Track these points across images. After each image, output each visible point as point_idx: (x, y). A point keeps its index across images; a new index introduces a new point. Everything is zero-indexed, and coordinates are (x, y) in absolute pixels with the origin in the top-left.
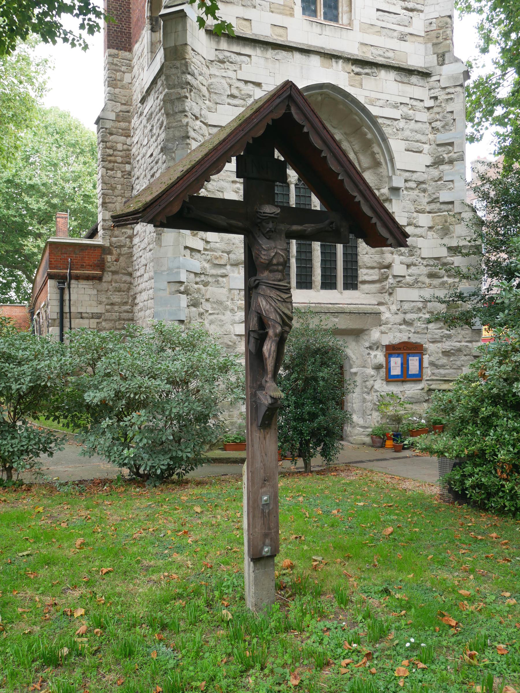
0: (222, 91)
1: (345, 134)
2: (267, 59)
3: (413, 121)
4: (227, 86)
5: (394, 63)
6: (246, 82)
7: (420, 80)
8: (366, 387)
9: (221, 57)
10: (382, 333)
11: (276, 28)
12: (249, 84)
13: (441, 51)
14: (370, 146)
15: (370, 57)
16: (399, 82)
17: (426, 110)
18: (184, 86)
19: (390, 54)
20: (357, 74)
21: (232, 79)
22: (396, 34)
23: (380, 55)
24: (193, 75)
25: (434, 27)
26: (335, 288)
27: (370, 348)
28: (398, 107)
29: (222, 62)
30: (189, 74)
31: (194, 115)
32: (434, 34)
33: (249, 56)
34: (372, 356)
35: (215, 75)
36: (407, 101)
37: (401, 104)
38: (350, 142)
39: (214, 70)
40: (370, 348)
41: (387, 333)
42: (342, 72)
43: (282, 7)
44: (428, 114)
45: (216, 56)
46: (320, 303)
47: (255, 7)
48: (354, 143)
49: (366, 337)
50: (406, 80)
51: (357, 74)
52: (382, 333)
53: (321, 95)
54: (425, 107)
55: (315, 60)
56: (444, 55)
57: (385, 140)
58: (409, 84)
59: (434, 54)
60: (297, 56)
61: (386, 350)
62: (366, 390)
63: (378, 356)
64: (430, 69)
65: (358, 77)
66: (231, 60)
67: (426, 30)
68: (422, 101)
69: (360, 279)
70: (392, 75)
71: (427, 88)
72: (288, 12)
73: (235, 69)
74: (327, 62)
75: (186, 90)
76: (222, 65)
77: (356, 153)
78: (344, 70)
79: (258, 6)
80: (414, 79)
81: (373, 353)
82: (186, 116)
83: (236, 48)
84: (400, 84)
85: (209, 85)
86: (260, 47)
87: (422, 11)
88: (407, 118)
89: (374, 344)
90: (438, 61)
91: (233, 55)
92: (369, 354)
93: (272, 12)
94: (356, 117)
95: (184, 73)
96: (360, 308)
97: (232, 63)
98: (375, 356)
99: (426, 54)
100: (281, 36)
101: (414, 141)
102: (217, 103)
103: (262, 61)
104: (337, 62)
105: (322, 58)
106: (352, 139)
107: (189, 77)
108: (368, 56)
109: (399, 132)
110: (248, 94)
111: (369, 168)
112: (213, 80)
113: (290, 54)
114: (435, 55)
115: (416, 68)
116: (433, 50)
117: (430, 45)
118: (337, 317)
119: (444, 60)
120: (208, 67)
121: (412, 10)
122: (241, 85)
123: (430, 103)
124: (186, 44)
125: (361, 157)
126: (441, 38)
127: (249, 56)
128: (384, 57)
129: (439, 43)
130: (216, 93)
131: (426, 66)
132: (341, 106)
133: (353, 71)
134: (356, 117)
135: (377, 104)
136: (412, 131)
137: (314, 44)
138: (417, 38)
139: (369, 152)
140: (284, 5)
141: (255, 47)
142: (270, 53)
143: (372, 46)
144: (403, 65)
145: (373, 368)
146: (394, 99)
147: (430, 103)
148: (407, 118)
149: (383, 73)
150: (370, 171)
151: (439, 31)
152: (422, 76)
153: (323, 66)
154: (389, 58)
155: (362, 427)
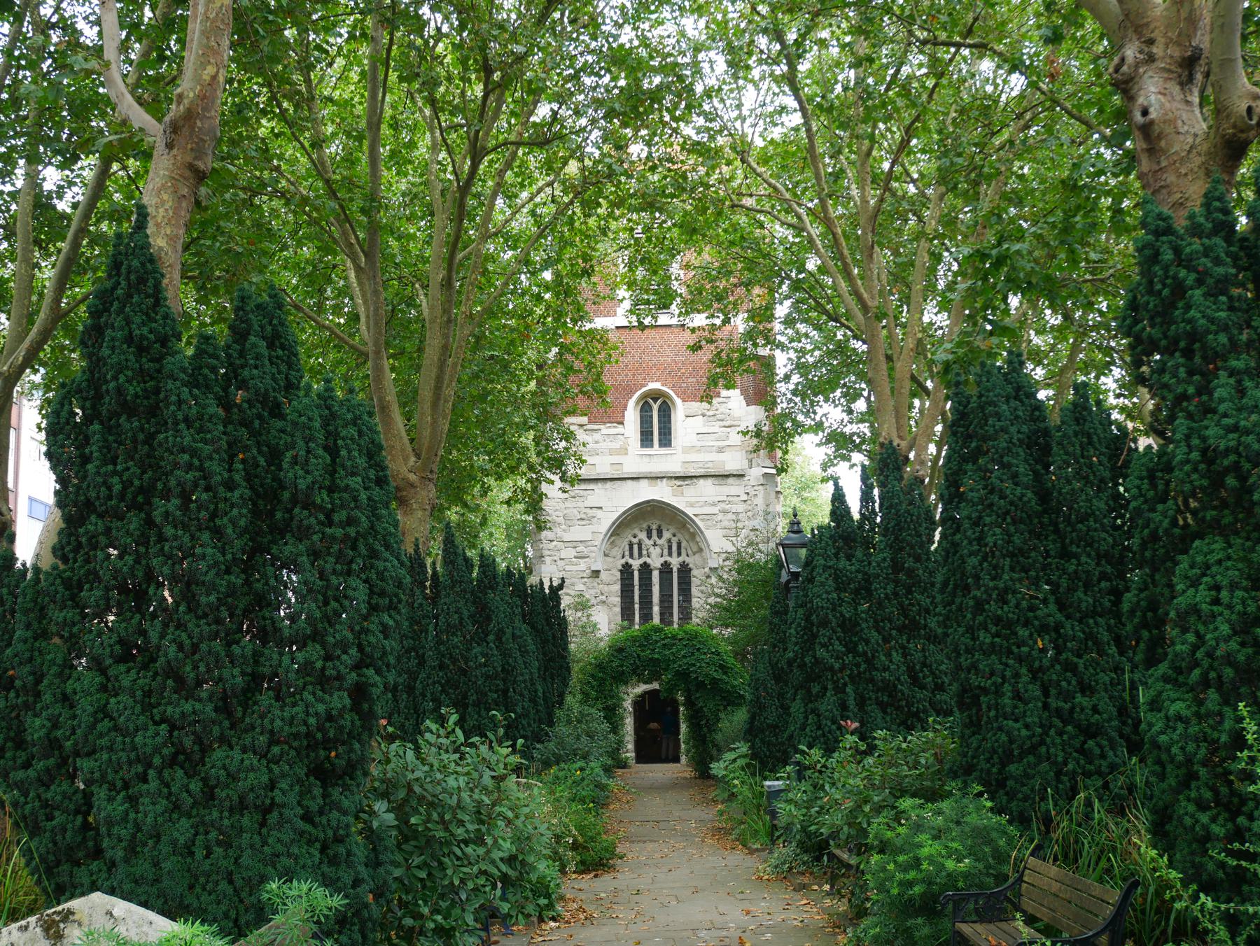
19: (710, 465)
39: (568, 504)
55: (644, 483)
60: (630, 482)
70: (710, 481)
74: (654, 482)
80: (731, 480)
88: (724, 512)
122: (588, 511)
123: (744, 497)
142: (609, 484)
146: (710, 500)
147: (744, 497)
148: (724, 512)
149: (702, 481)
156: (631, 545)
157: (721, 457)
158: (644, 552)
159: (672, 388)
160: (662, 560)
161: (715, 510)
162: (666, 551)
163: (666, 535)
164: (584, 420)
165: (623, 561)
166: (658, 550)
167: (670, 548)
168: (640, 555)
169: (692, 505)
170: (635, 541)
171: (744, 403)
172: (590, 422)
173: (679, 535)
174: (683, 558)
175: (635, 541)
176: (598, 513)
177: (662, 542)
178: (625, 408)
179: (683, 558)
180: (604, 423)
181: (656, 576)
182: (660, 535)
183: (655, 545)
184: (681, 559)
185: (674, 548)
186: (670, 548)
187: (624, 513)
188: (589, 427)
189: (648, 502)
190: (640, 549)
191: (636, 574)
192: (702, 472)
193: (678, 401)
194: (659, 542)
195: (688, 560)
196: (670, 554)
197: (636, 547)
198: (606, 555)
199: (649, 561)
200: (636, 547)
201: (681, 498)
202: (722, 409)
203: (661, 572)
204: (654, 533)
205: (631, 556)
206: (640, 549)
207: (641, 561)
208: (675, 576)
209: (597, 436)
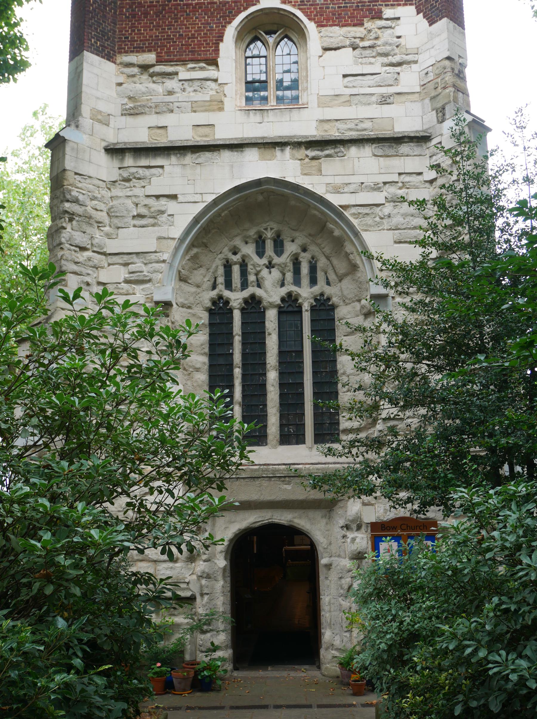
0: (125, 212)
1: (310, 235)
2: (184, 165)
3: (406, 204)
4: (131, 206)
5: (372, 134)
6: (158, 197)
7: (415, 148)
8: (342, 588)
9: (125, 175)
10: (364, 504)
11: (200, 129)
12: (161, 198)
13: (439, 105)
14: (342, 246)
15: (334, 134)
16: (381, 156)
17: (427, 185)
18: (62, 216)
19: (367, 125)
20: (313, 158)
21: (139, 197)
22: (374, 99)
23: (351, 129)
24: (76, 201)
25: (431, 76)
26: (304, 442)
27: (347, 527)
28: (380, 188)
29: (128, 180)
30: (68, 201)
31: (76, 246)
32: (431, 86)
33: (162, 167)
34: (349, 540)
35: (117, 196)
36: (395, 178)
37: (385, 183)
38: (318, 245)
39: (116, 191)
40: (347, 527)
41: (372, 505)
42: (291, 161)
43: (207, 104)
44: (432, 188)
45: (120, 175)
46: (268, 465)
47: (172, 111)
48: (323, 246)
49: (340, 512)
50: (391, 152)
51: (313, 158)
52: (364, 504)
53: (262, 193)
54: (426, 182)
55: (251, 154)
56: (444, 109)
57: (357, 234)
58: (397, 156)
59: (433, 110)
60: (226, 154)
61: (372, 531)
62: (342, 591)
63: (358, 540)
64: (429, 131)
65: (315, 163)
66: (138, 176)
67: (422, 83)
68: (420, 174)
69: (341, 427)
70: (368, 150)
71: (428, 156)
72: (216, 107)
73: (143, 184)
74: (268, 152)
75: (63, 220)
76: (127, 184)
77: (328, 258)
78: (293, 158)
79: (176, 109)
80: (404, 148)
81: (350, 535)
82: (62, 248)
83: (144, 162)
84: (381, 159)
85: (109, 209)
86: (175, 154)
87: (416, 62)
89: (353, 521)
90: (437, 118)
91: (140, 171)
92: (344, 537)
93: (195, 112)
94: (316, 212)
95: (62, 201)
96: (328, 468)
97: (139, 179)
98: (354, 540)
99: (424, 113)
100: (206, 136)
101: (410, 229)
102: (119, 228)
103: (178, 170)
104: (282, 150)
105: (262, 150)
106: (319, 241)
107: (67, 205)
108: (332, 133)
109: (384, 221)
110: (159, 211)
111: (346, 275)
112: (115, 202)
113: (216, 154)
114: (434, 112)
115: (406, 134)
116: (432, 105)
117: (427, 101)
118: (289, 483)
119: (444, 115)
120: (109, 189)
121: (399, 64)
122: (152, 202)
123: (433, 174)
124: (65, 170)
125: (335, 262)
126: (439, 88)
127: (162, 167)
128: (358, 130)
129: (437, 95)
130: (117, 216)
131: (425, 127)
132: (293, 203)
133: (307, 156)
134: (316, 212)
135: (346, 190)
136: (405, 215)
137: (251, 135)
138: (410, 97)
139: (343, 253)
140: (210, 101)
141: (169, 155)
142: (189, 158)
143: (337, 120)
144: (388, 134)
145: (352, 559)
146: (369, 180)
147: (433, 174)
149: (353, 151)
150: (349, 278)
151: (437, 80)
152: (418, 142)
153: (262, 158)
154: (365, 130)
155: (338, 650)
156: (228, 267)
157: (387, 111)
158: (252, 278)
159: (300, 6)
160: (283, 291)
161: (378, 198)
162: (289, 276)
163: (291, 248)
164: (150, 57)
165: (214, 294)
166: (276, 274)
167: (297, 271)
168: (244, 285)
169: (337, 190)
170: (236, 258)
171: (425, 22)
172: (160, 61)
173: (313, 249)
174: (321, 287)
175: (235, 258)
176: (171, 206)
177: (285, 259)
178: (220, 38)
179: (321, 287)
180: (183, 62)
181: (272, 316)
182: (279, 247)
183: (270, 266)
184: (316, 289)
185: (305, 270)
186: (297, 271)
187: (215, 202)
188: (158, 69)
189: (258, 183)
190: (244, 273)
191: (237, 315)
192: (353, 135)
193: (310, 27)
194: (276, 260)
195: (328, 291)
196: (297, 282)
197: (236, 269)
198: (183, 279)
199: (259, 292)
200: (236, 269)
201: (315, 179)
202: (386, 36)
203: (281, 313)
204: (269, 245)
205: (228, 285)
206: (244, 273)
207: (246, 294)
208: (306, 317)
209: (171, 84)
